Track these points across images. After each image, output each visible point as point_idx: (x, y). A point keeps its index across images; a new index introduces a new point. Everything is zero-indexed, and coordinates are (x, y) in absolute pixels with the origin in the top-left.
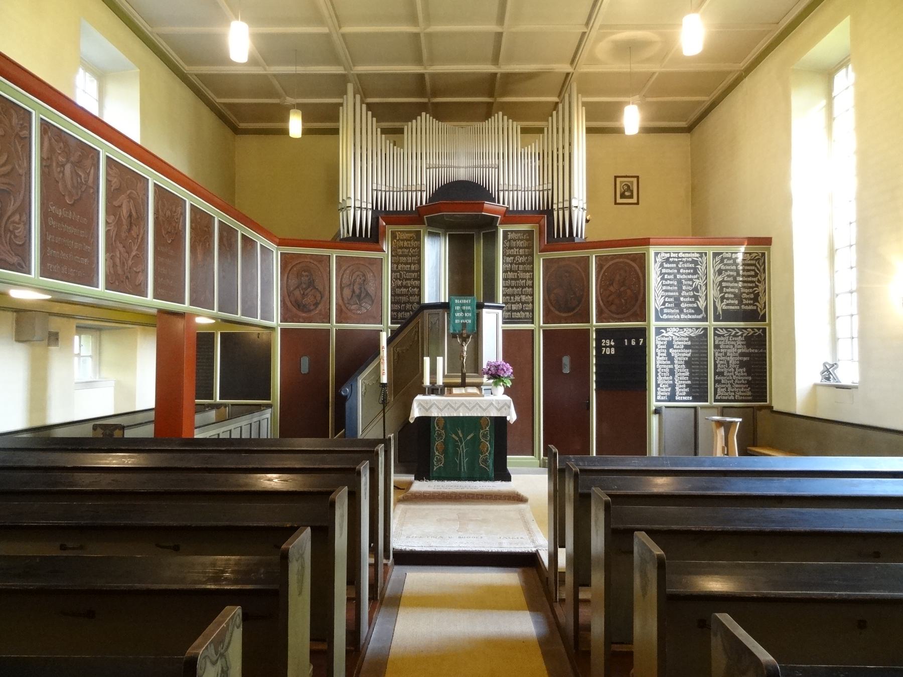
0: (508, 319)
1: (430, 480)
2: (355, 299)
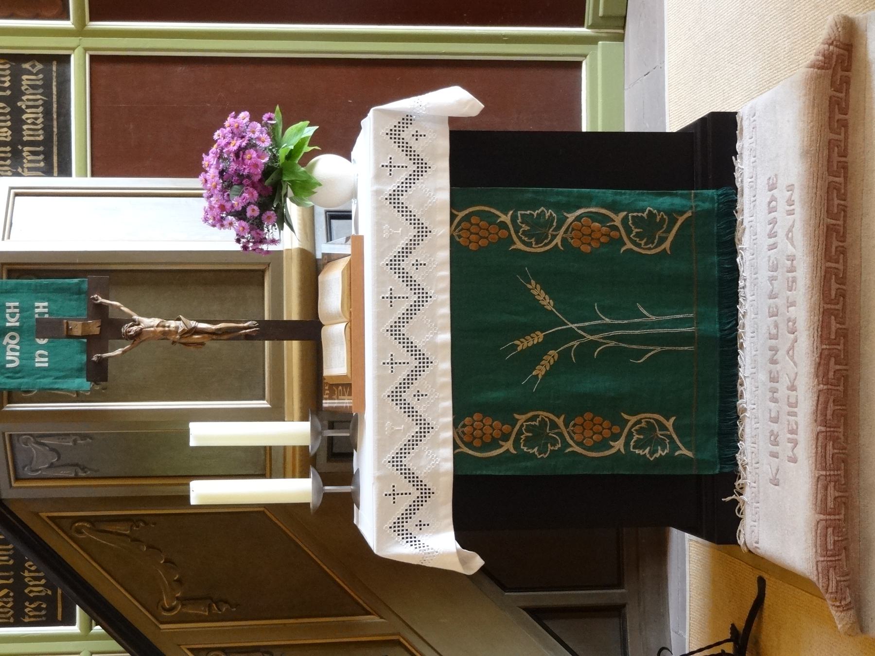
0: (48, 159)
1: (735, 475)
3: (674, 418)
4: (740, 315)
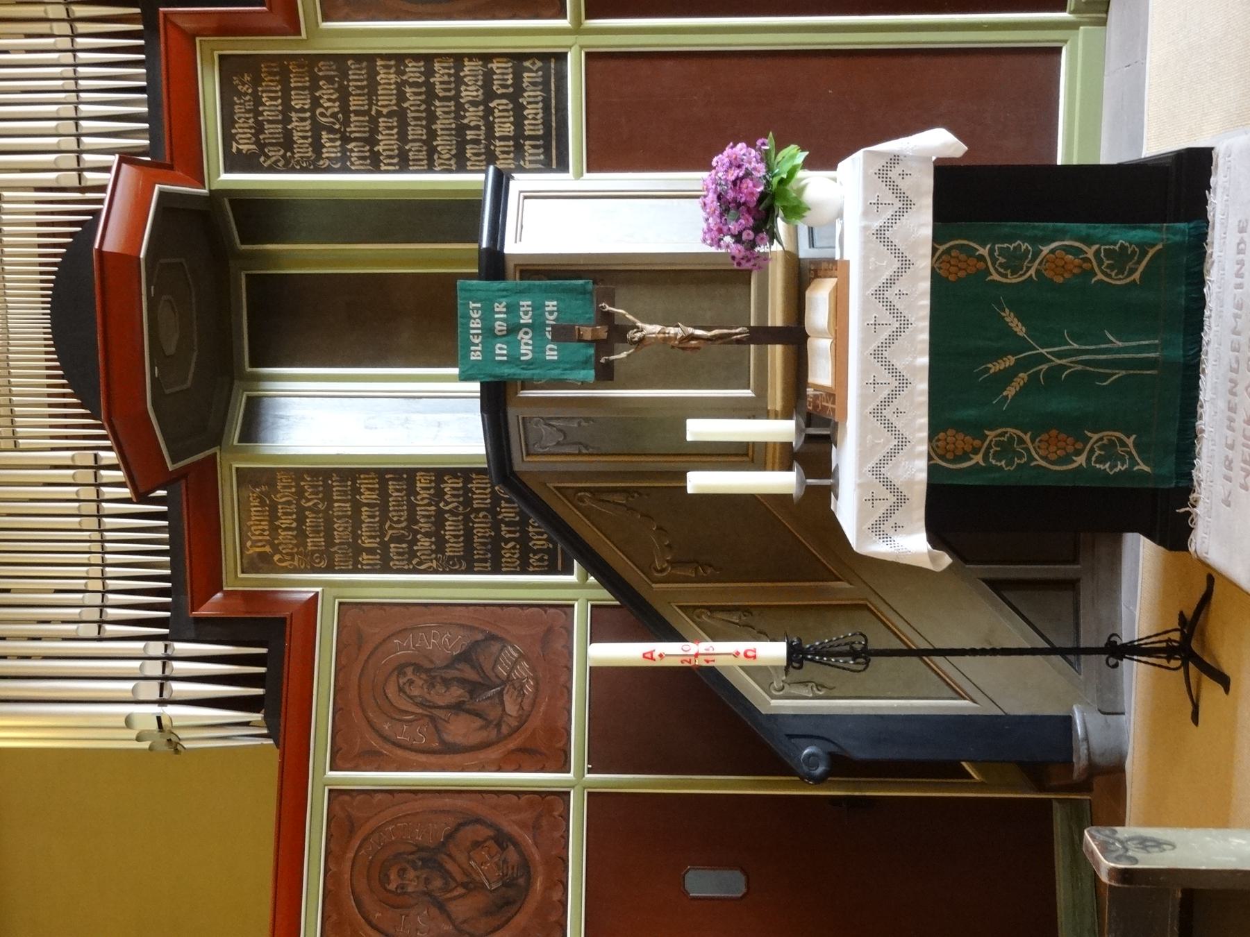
1: (1190, 489)
2: (481, 703)
3: (1134, 436)
4: (1204, 343)
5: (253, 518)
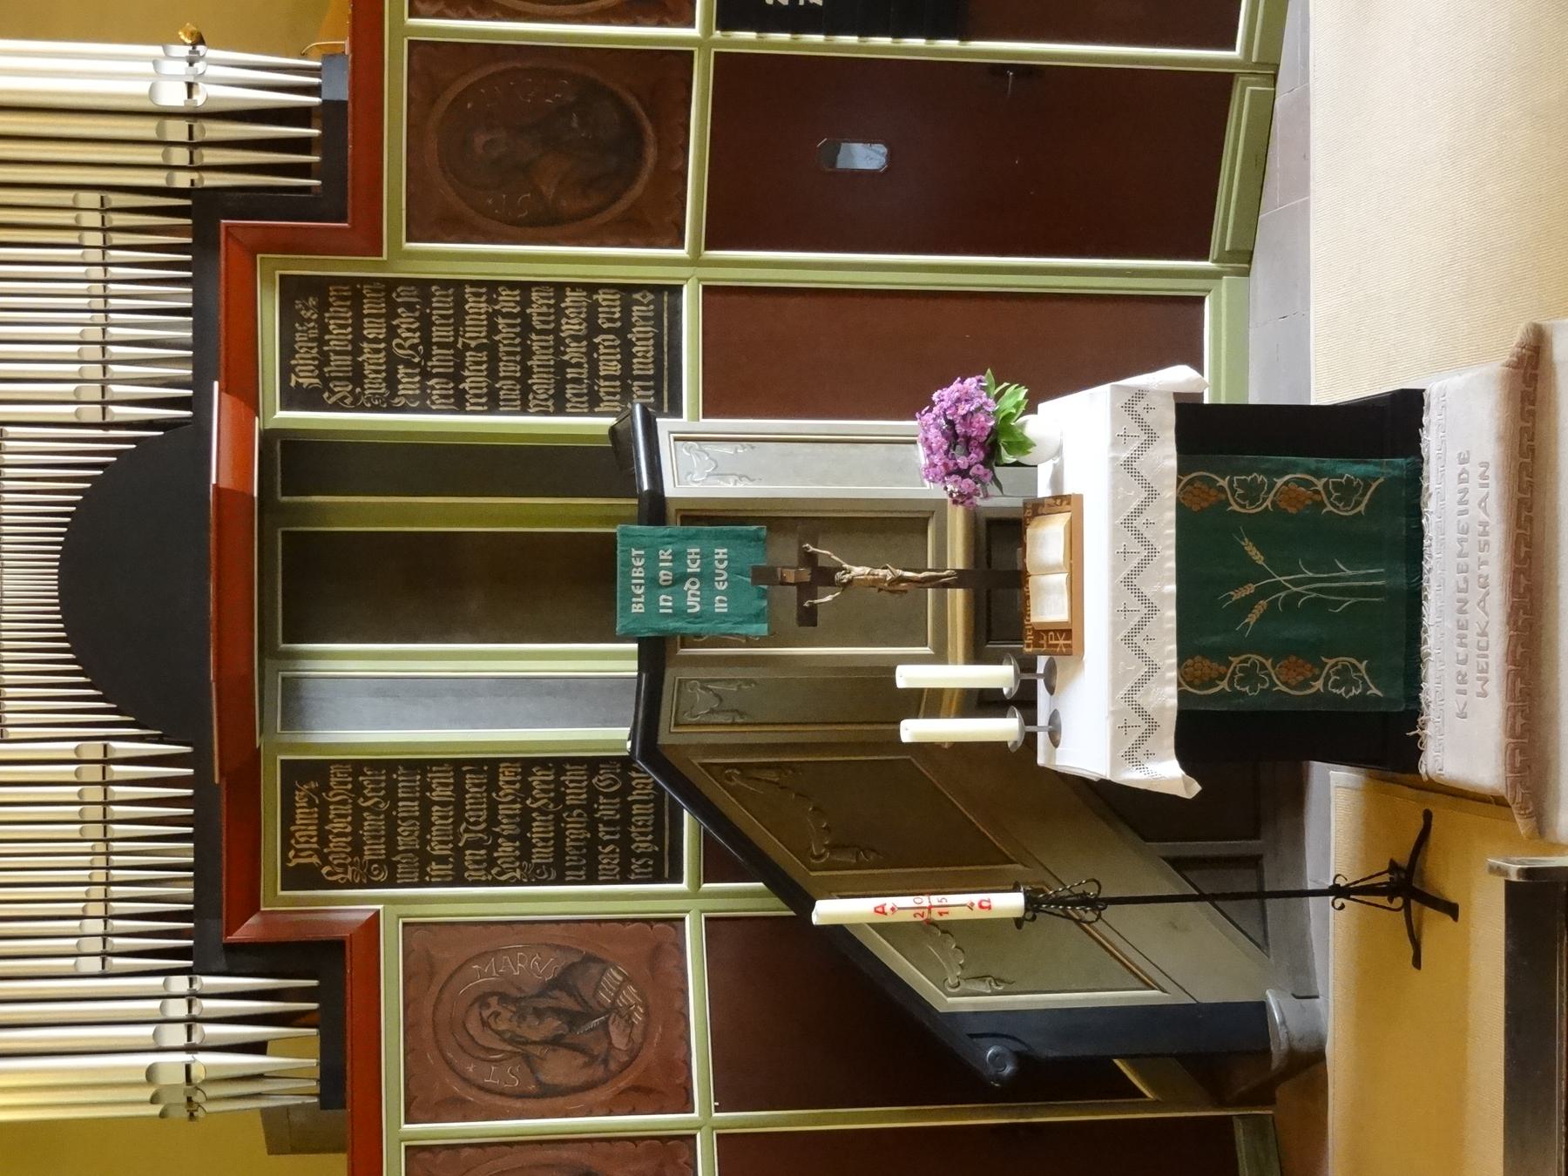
2: (584, 1032)
4: (1425, 571)
5: (298, 822)
